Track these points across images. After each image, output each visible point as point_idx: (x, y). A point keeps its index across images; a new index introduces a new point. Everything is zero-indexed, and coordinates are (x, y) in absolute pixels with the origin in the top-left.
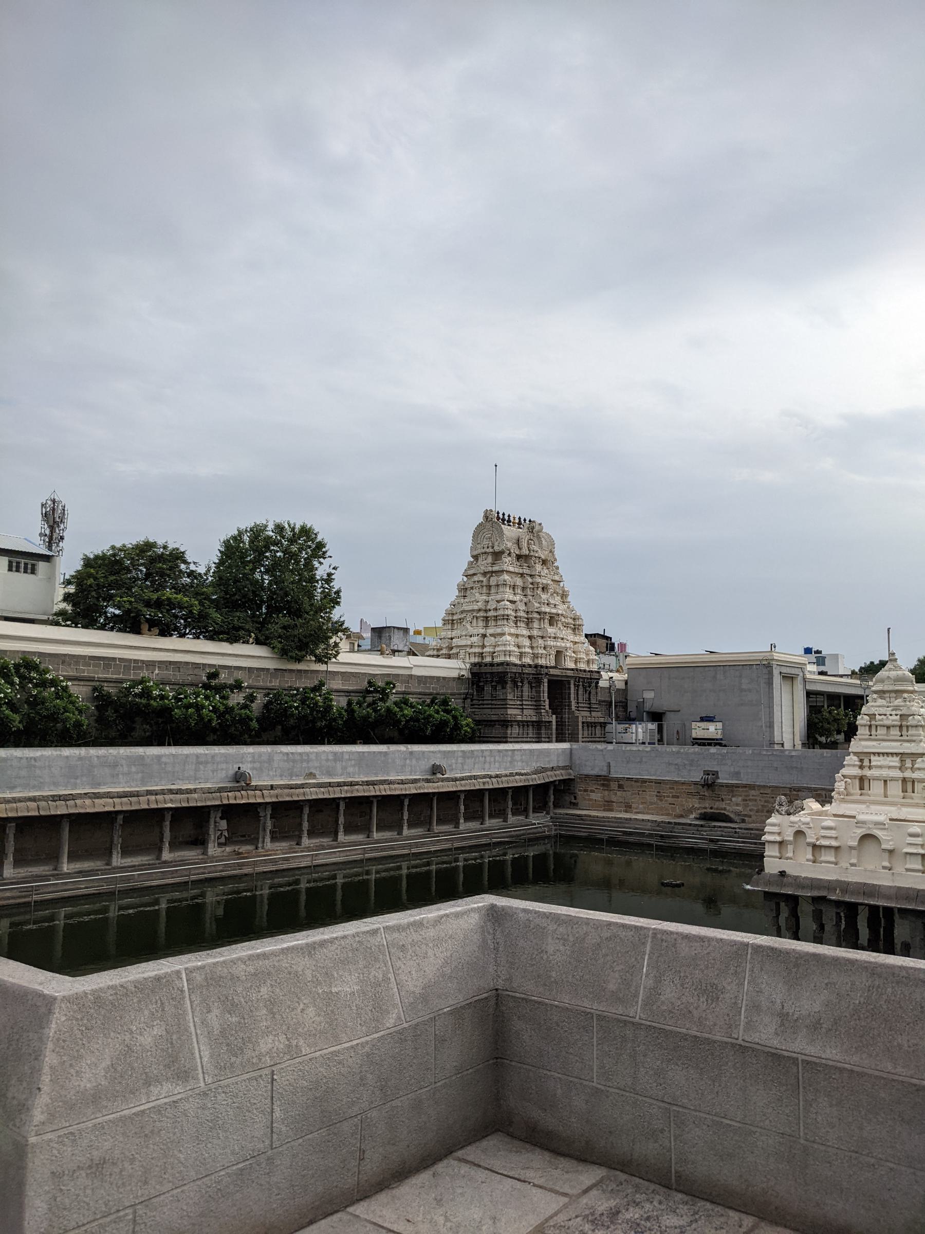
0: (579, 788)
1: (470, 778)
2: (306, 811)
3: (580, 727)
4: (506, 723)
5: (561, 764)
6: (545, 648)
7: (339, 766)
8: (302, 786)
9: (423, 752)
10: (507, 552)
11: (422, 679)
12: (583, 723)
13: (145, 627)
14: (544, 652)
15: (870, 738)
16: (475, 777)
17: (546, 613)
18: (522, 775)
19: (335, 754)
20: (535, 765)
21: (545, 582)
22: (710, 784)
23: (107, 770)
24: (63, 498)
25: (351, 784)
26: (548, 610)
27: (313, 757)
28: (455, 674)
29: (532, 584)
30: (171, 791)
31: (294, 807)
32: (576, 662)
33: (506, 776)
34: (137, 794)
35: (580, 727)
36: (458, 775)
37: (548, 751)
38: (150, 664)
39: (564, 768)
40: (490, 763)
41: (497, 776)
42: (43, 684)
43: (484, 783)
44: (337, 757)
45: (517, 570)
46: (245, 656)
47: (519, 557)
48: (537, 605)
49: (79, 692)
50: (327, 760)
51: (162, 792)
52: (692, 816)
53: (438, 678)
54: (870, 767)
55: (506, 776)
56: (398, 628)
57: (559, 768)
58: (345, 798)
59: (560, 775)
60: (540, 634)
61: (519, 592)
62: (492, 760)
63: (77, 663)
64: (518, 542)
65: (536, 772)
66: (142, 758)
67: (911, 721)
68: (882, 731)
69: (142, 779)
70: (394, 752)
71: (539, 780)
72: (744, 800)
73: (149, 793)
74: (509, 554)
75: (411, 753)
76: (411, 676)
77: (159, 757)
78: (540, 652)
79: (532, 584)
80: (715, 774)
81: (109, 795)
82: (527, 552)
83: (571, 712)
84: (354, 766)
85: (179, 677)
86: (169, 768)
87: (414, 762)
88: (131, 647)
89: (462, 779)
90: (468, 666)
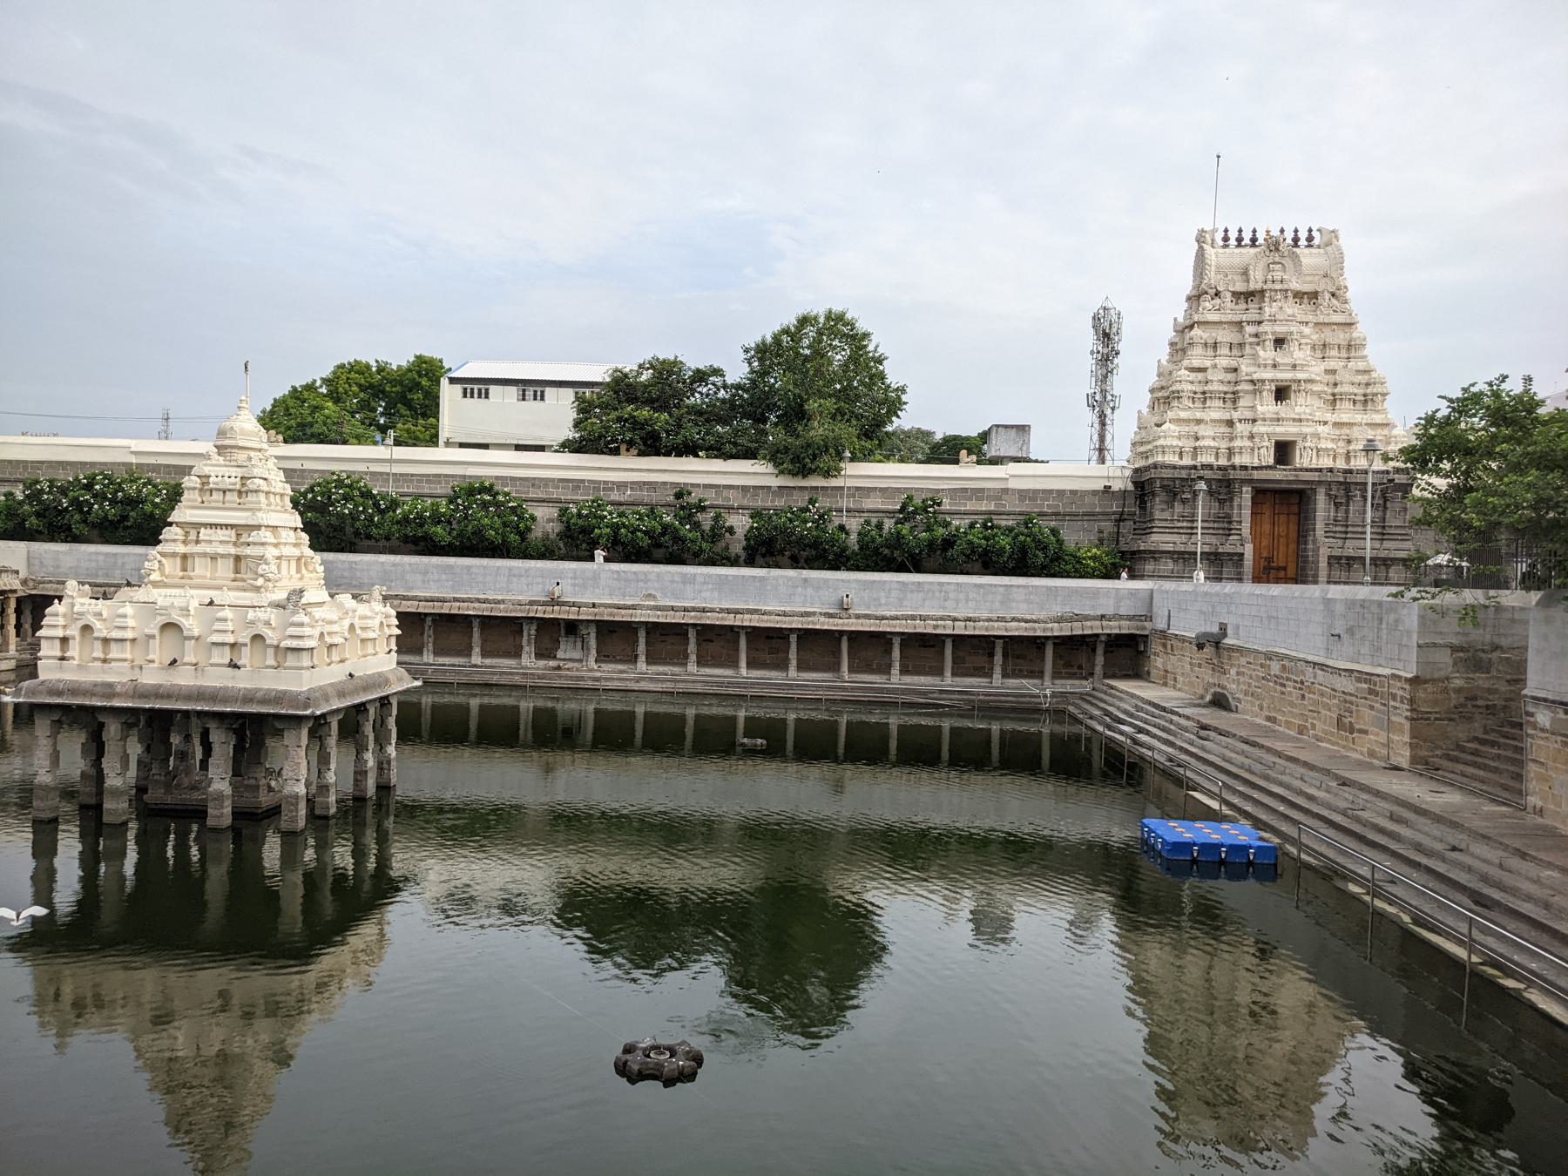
0: (1155, 646)
1: (913, 618)
2: (642, 635)
3: (1323, 564)
4: (1155, 555)
5: (1123, 612)
6: (1251, 437)
7: (689, 588)
8: (633, 607)
9: (826, 581)
10: (1260, 292)
11: (1023, 494)
12: (1330, 557)
13: (623, 447)
14: (1247, 443)
15: (202, 505)
16: (922, 618)
17: (1263, 381)
18: (1027, 621)
19: (684, 575)
20: (1058, 610)
21: (1281, 329)
22: (1213, 643)
23: (419, 577)
24: (1116, 303)
25: (704, 610)
26: (1268, 375)
27: (652, 577)
28: (1099, 486)
29: (1256, 335)
30: (478, 600)
31: (629, 629)
32: (1348, 457)
33: (990, 620)
34: (444, 600)
35: (1323, 564)
36: (888, 614)
37: (1096, 593)
38: (621, 486)
39: (1131, 618)
40: (957, 601)
41: (970, 619)
42: (485, 505)
43: (935, 627)
44: (686, 580)
45: (1230, 318)
46: (754, 473)
47: (1248, 296)
48: (1252, 369)
49: (854, 524)
50: (673, 582)
51: (470, 600)
52: (1208, 698)
53: (1061, 493)
54: (197, 542)
55: (990, 620)
56: (1006, 427)
57: (1121, 617)
58: (694, 625)
59: (1126, 628)
60: (1249, 415)
61: (1225, 351)
62: (962, 596)
63: (546, 486)
64: (1245, 273)
65: (1059, 620)
66: (451, 567)
67: (251, 485)
68: (217, 496)
69: (453, 587)
70: (775, 578)
71: (1057, 630)
72: (1238, 673)
73: (456, 600)
74: (1217, 294)
75: (805, 580)
76: (1006, 491)
77: (469, 568)
78: (1237, 443)
79: (1256, 335)
80: (1223, 628)
81: (414, 598)
82: (1259, 286)
83: (1314, 541)
84: (712, 590)
85: (655, 498)
86: (480, 579)
87: (810, 591)
88: (600, 469)
89: (896, 618)
90: (1128, 473)
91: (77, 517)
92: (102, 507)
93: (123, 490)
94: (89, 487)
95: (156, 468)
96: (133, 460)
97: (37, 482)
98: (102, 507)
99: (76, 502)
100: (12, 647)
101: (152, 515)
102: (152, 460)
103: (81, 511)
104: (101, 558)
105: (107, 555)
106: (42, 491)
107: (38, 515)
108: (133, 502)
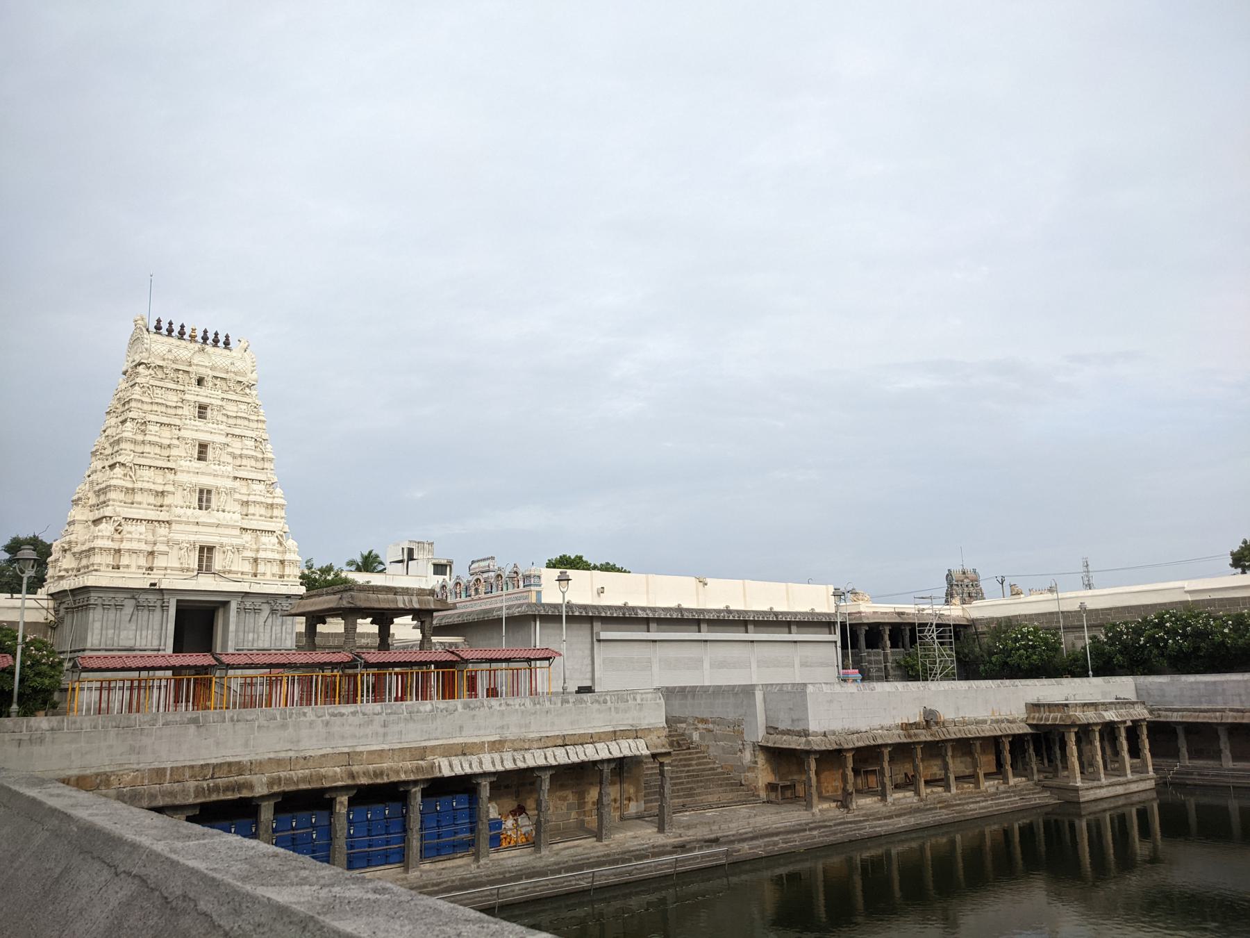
91: (1155, 651)
92: (1176, 642)
93: (1190, 625)
94: (1160, 625)
95: (1211, 602)
96: (1189, 598)
97: (1114, 625)
98: (1176, 642)
99: (1151, 639)
100: (1150, 768)
101: (1223, 643)
102: (1206, 597)
103: (1158, 646)
104: (1202, 686)
105: (1206, 683)
106: (1121, 633)
107: (1120, 652)
108: (1201, 634)
